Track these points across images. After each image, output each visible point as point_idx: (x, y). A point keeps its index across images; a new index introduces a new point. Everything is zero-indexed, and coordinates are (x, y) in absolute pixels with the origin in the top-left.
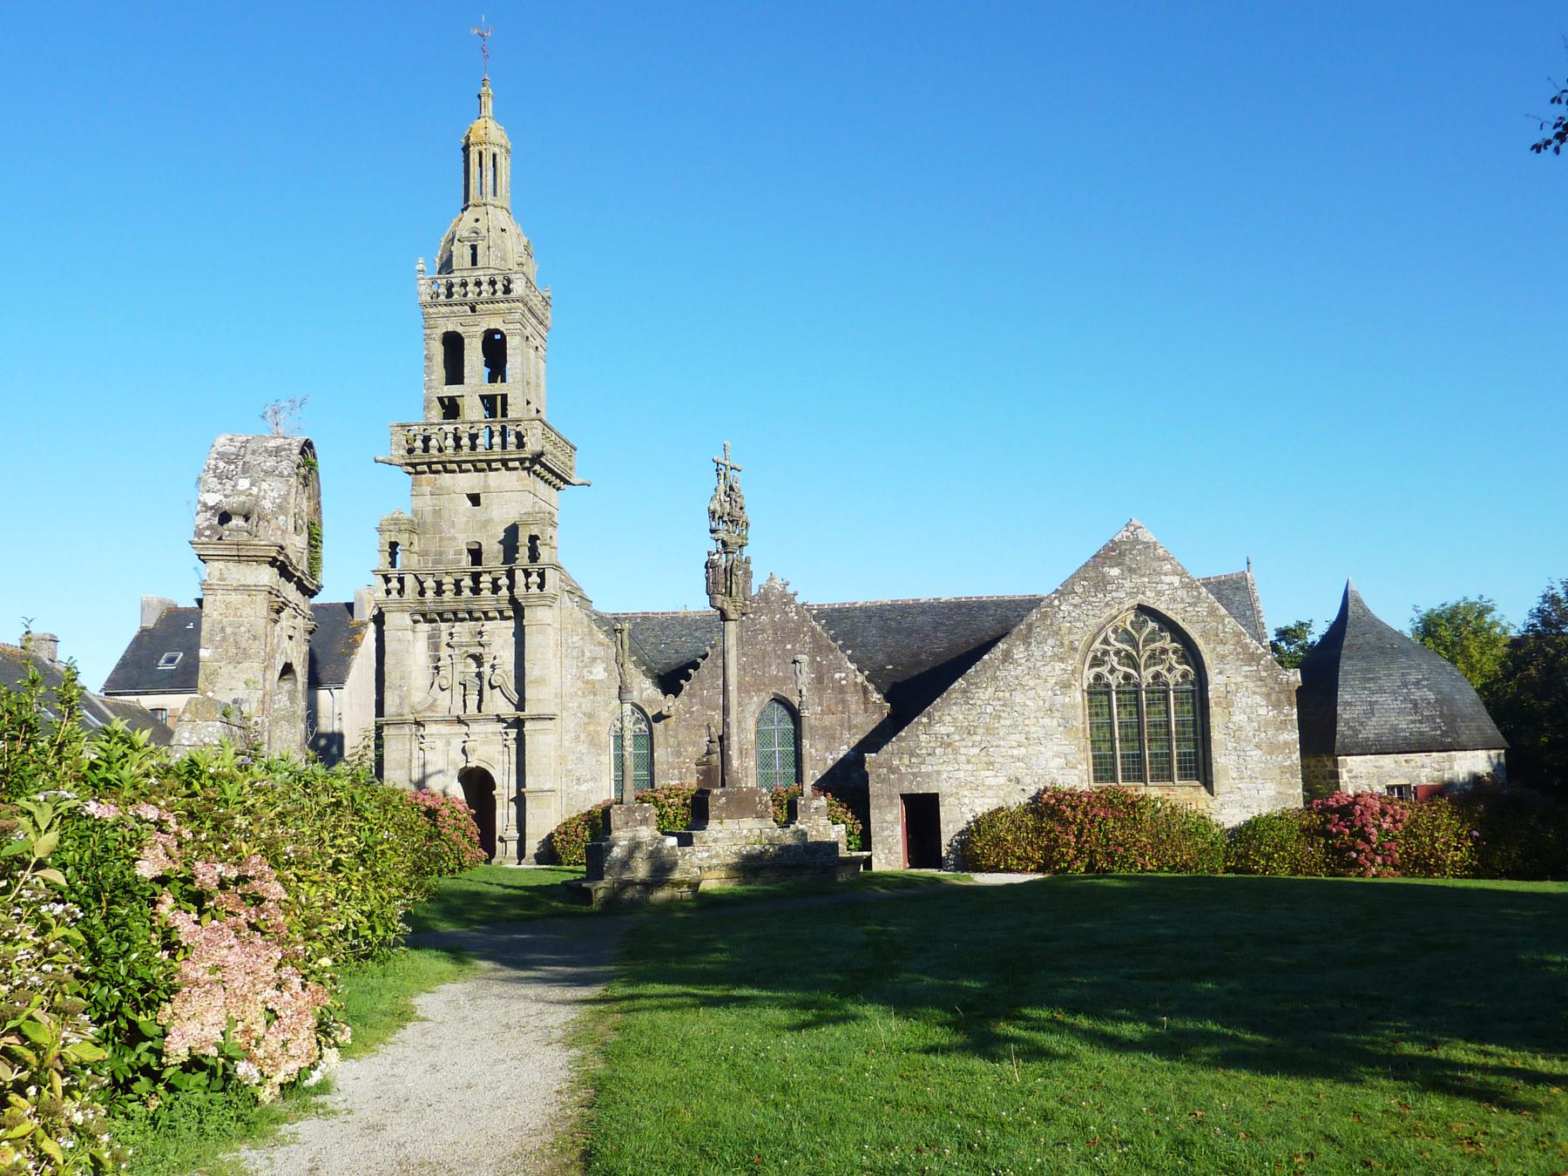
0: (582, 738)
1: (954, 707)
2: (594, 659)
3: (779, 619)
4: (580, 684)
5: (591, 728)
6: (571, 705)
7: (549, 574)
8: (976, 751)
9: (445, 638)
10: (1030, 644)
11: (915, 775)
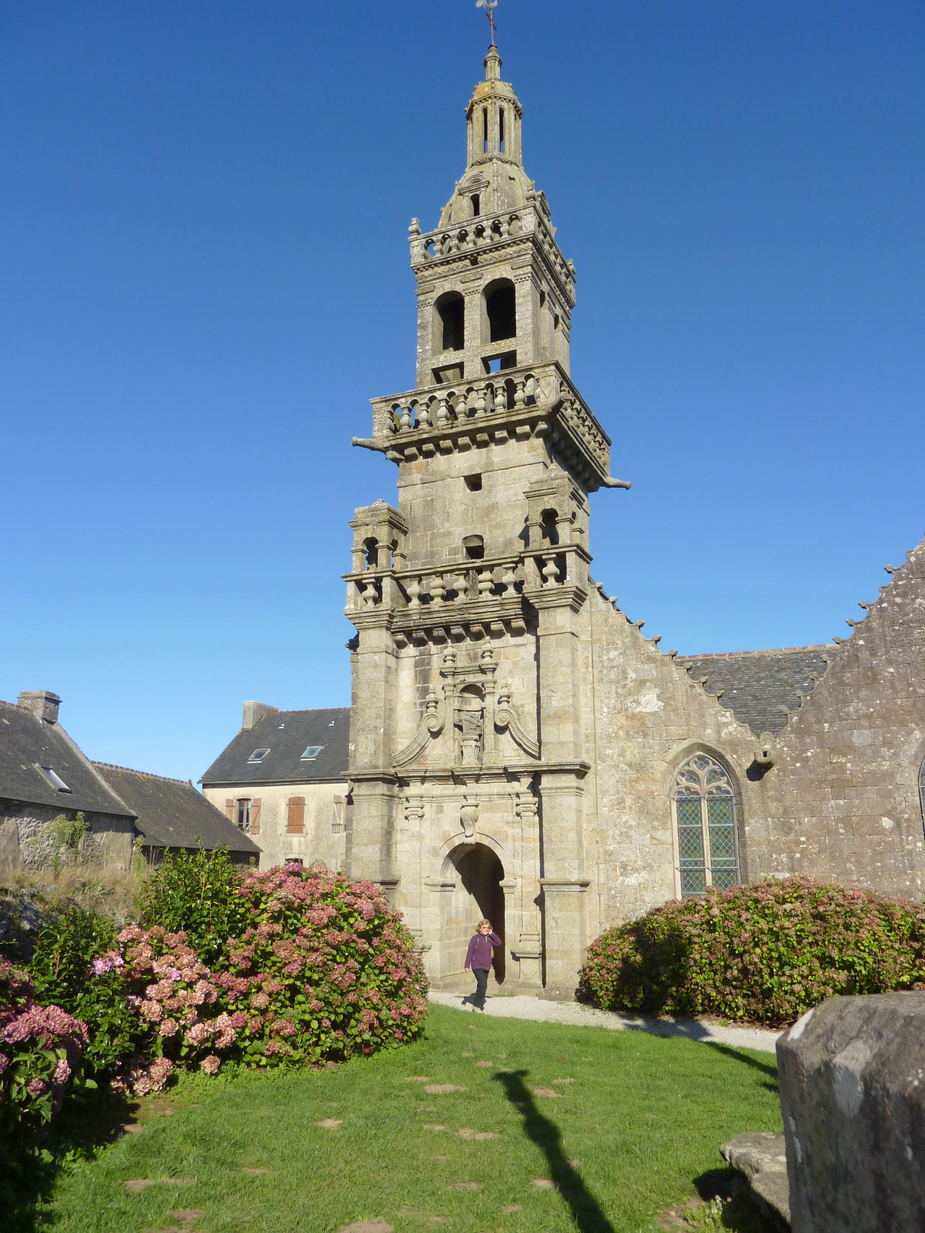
0: (629, 801)
2: (642, 683)
4: (622, 720)
5: (642, 787)
6: (609, 752)
7: (572, 560)
9: (436, 664)
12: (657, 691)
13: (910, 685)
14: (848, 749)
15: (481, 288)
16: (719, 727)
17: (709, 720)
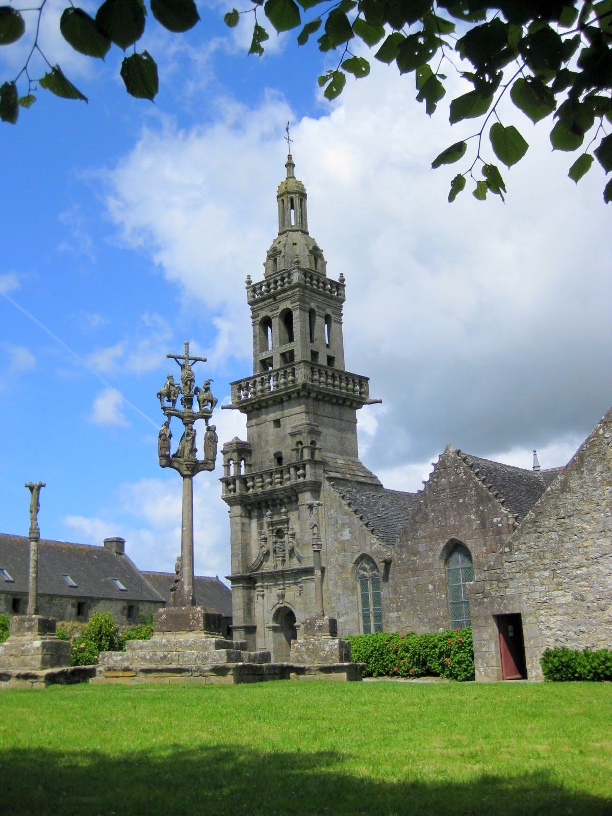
1: (527, 536)
2: (343, 525)
3: (454, 479)
4: (336, 544)
5: (344, 576)
6: (332, 560)
8: (546, 573)
10: (582, 472)
11: (502, 597)
12: (349, 529)
13: (439, 521)
14: (416, 553)
15: (278, 314)
16: (371, 545)
17: (368, 542)
